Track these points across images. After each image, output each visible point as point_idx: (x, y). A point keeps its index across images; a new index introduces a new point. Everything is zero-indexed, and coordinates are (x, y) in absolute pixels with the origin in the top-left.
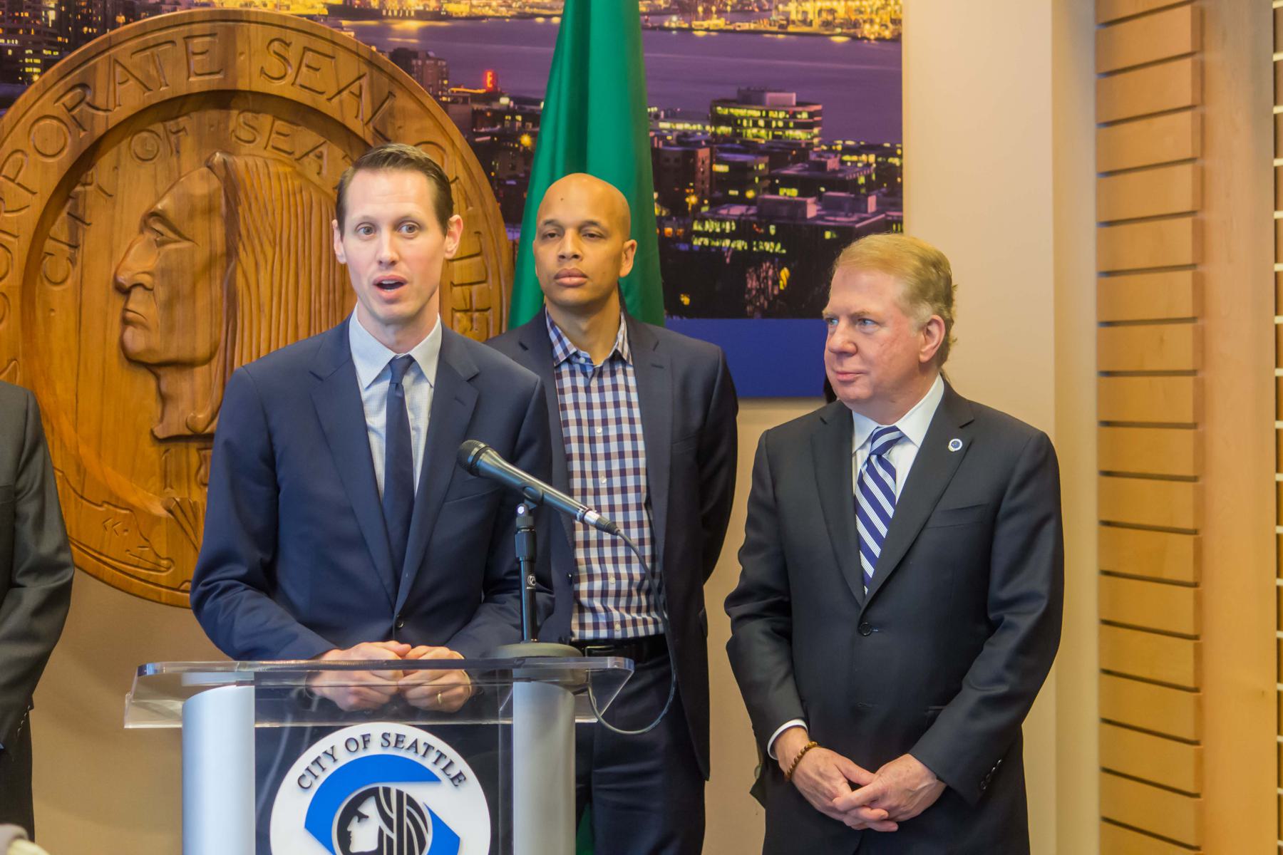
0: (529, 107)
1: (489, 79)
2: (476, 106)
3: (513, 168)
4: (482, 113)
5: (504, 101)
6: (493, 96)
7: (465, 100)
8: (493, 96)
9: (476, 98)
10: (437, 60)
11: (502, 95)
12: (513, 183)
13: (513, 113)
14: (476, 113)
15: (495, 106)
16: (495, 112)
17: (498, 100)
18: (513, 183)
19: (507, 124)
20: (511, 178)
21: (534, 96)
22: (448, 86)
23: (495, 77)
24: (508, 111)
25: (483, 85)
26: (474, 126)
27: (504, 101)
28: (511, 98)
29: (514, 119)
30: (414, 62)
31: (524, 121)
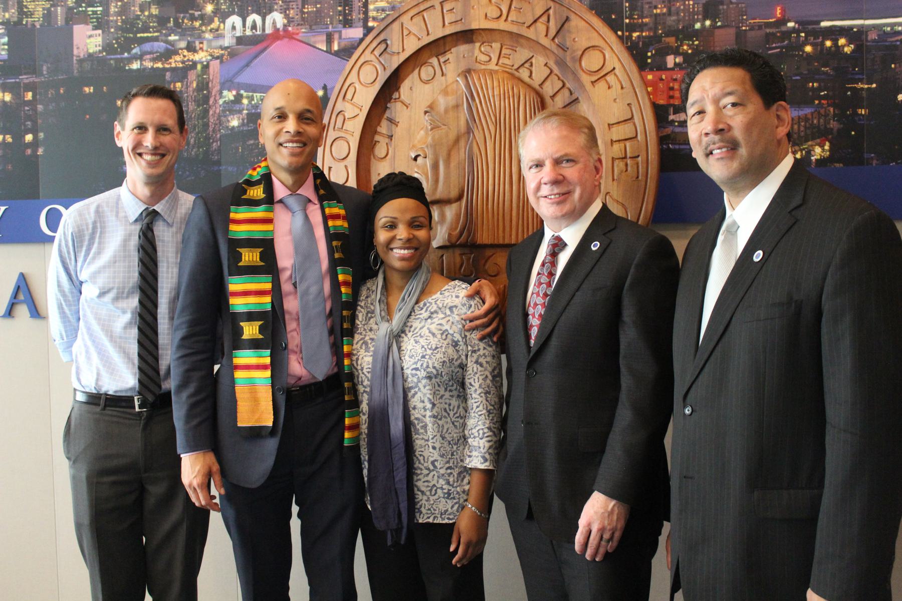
0: (810, 27)
1: (779, 11)
2: (768, 31)
3: (798, 68)
4: (773, 34)
5: (791, 24)
6: (783, 21)
7: (760, 27)
8: (783, 21)
9: (768, 25)
10: (737, 4)
11: (789, 21)
12: (798, 78)
13: (797, 32)
14: (767, 35)
15: (783, 29)
16: (783, 33)
17: (786, 24)
18: (798, 78)
19: (793, 40)
20: (797, 75)
21: (815, 19)
22: (746, 20)
23: (783, 11)
24: (793, 30)
25: (775, 16)
26: (768, 42)
27: (791, 24)
28: (796, 23)
29: (799, 36)
30: (721, 7)
31: (806, 37)
